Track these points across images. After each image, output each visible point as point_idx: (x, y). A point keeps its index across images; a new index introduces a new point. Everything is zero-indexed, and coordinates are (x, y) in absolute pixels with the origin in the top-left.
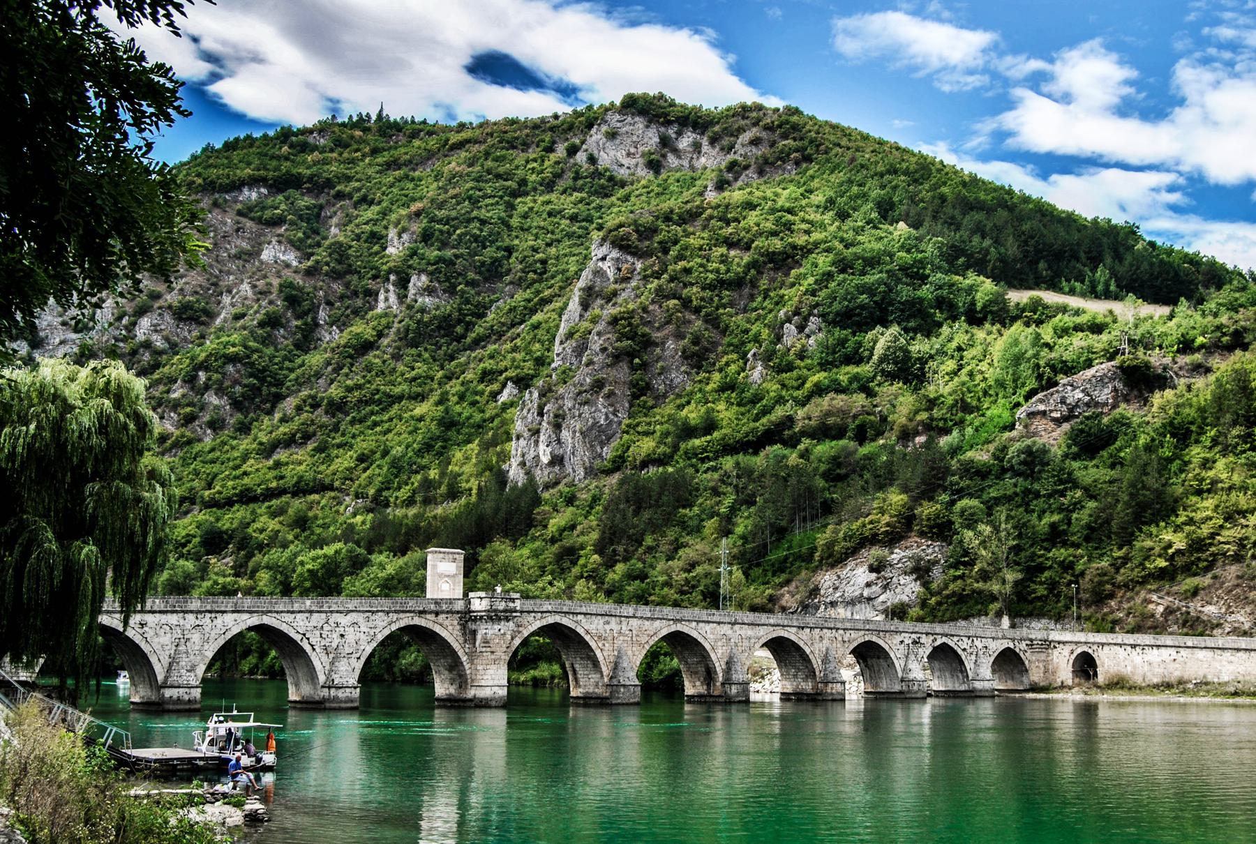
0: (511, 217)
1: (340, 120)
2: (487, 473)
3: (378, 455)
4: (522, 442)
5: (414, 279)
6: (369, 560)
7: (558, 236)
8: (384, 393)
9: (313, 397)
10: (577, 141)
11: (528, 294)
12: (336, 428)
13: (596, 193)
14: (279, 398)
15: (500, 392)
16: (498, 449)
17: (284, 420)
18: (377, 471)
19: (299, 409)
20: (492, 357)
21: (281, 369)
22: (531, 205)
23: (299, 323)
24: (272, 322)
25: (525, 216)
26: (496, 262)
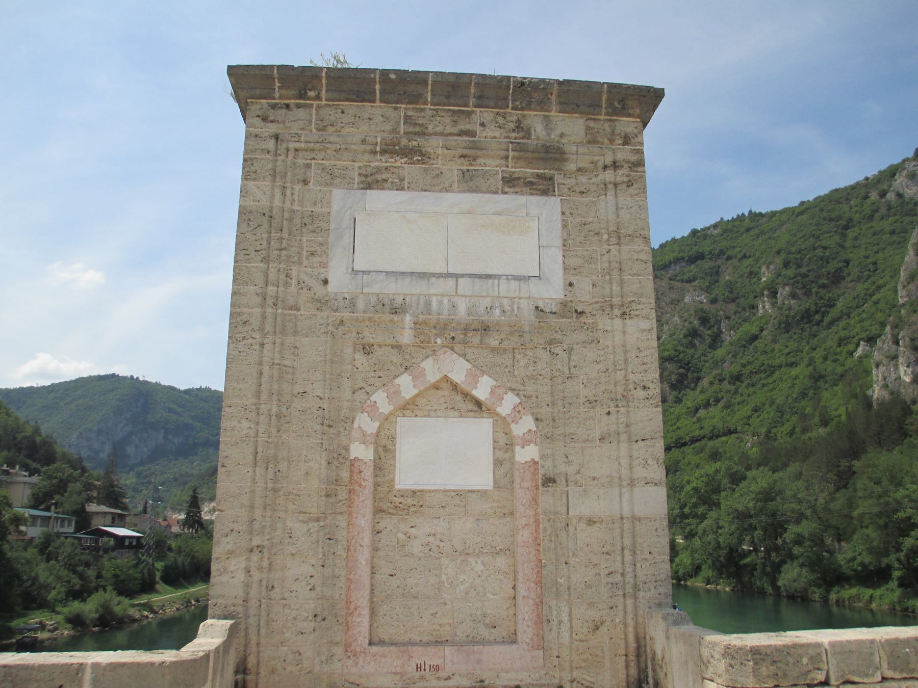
0: (845, 241)
1: (726, 219)
2: (853, 400)
3: (767, 406)
4: (882, 368)
5: (780, 290)
6: (746, 475)
7: (883, 246)
8: (768, 365)
9: (720, 375)
10: (885, 187)
11: (866, 285)
12: (736, 392)
13: (907, 214)
14: (698, 379)
15: (856, 350)
16: (860, 382)
17: (702, 392)
18: (766, 416)
19: (711, 383)
20: (844, 329)
21: (700, 361)
22: (859, 231)
23: (709, 332)
24: (693, 334)
25: (856, 239)
26: (839, 270)
